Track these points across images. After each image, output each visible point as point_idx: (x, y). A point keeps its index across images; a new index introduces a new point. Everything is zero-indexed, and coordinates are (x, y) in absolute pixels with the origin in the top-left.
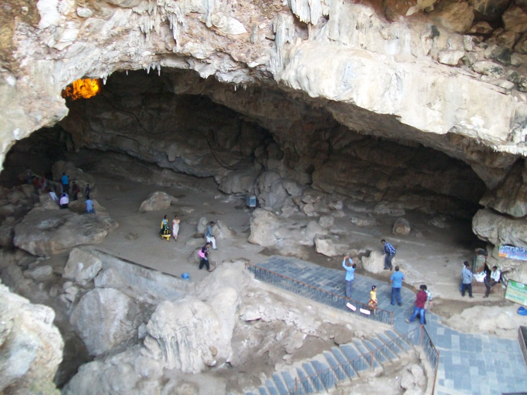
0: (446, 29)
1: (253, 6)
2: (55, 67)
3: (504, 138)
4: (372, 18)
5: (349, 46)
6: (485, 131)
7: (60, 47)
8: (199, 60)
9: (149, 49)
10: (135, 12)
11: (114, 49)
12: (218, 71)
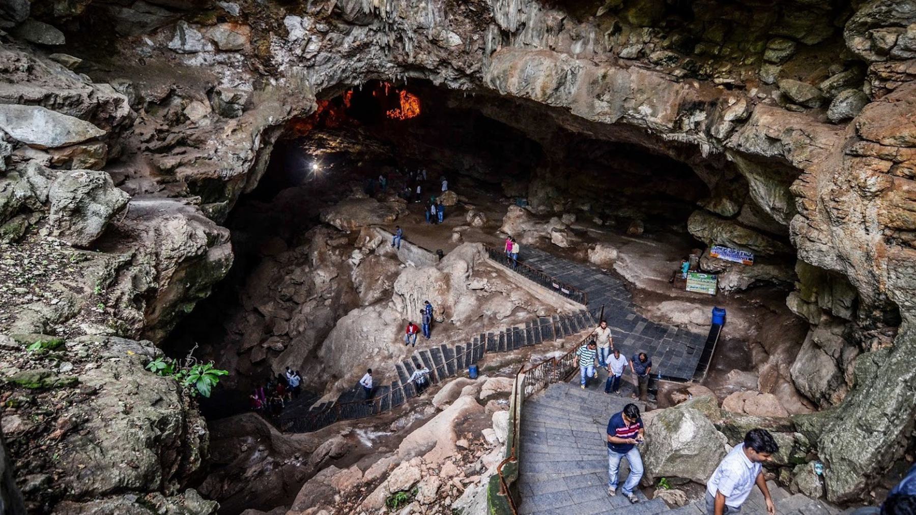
0: (630, 24)
1: (467, 21)
2: (308, 73)
3: (670, 125)
4: (565, 22)
5: (539, 48)
6: (652, 119)
7: (308, 56)
8: (430, 70)
9: (391, 61)
10: (370, 29)
11: (359, 60)
12: (446, 79)
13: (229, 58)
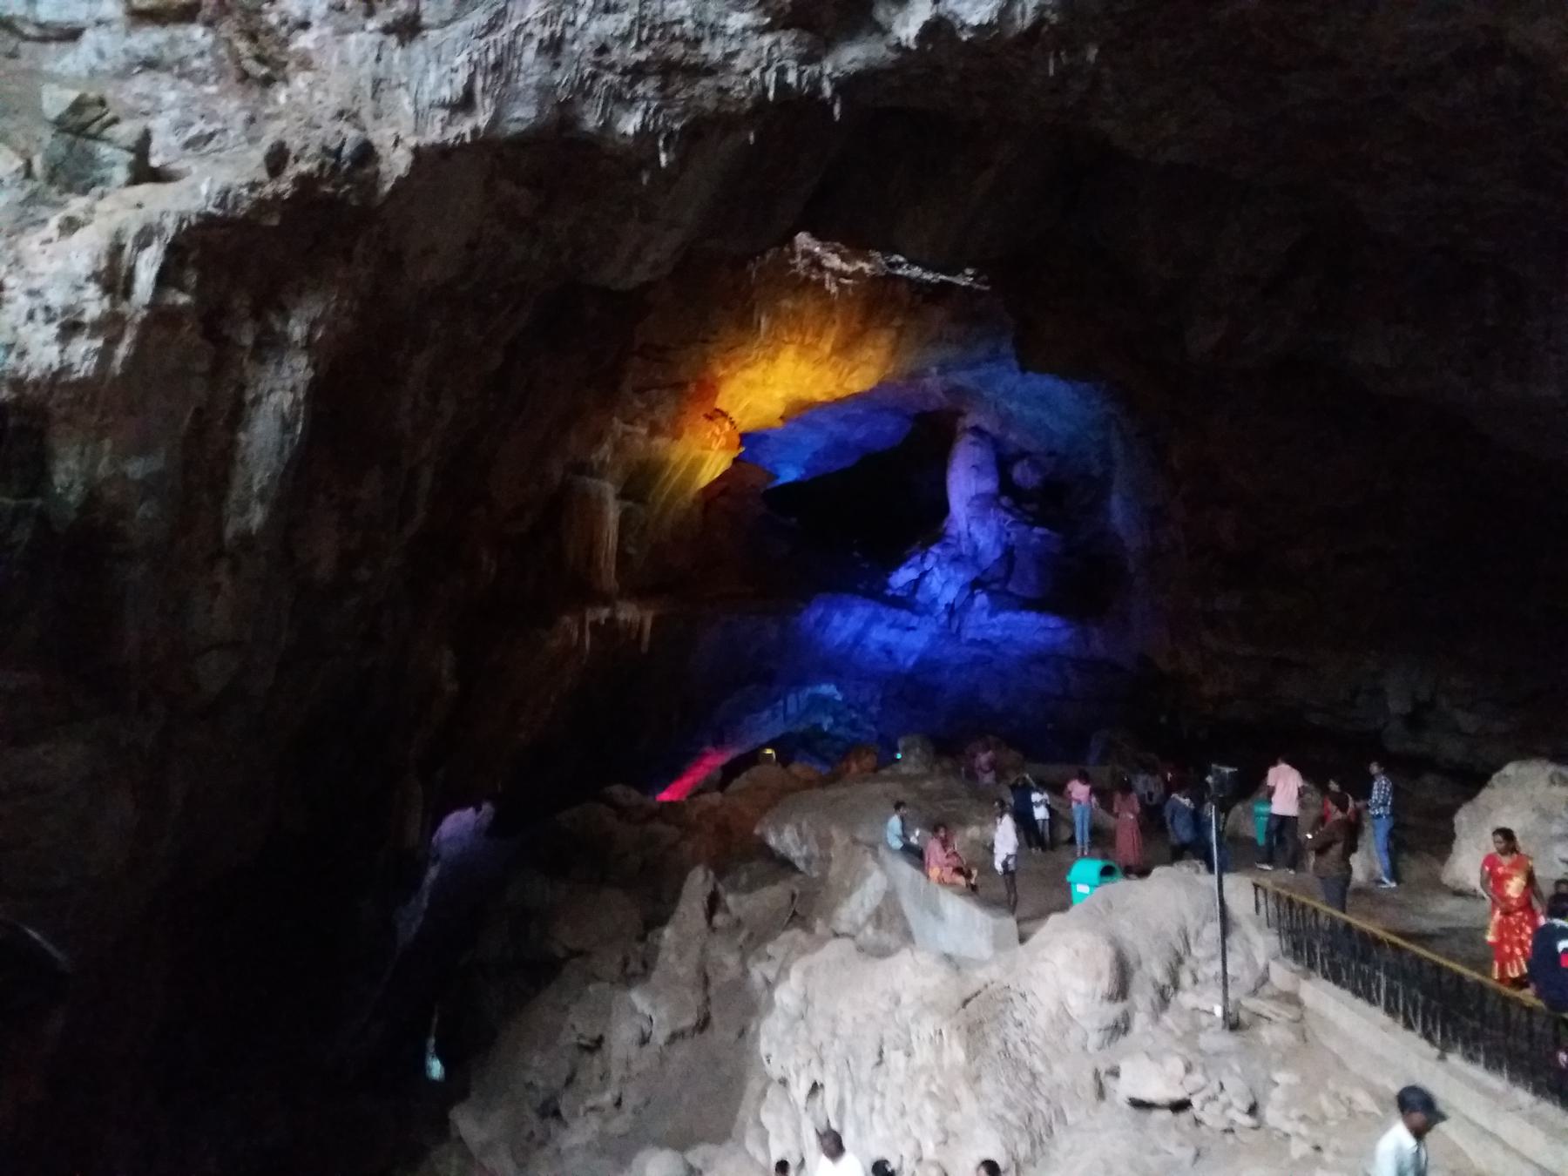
13: (173, 42)
